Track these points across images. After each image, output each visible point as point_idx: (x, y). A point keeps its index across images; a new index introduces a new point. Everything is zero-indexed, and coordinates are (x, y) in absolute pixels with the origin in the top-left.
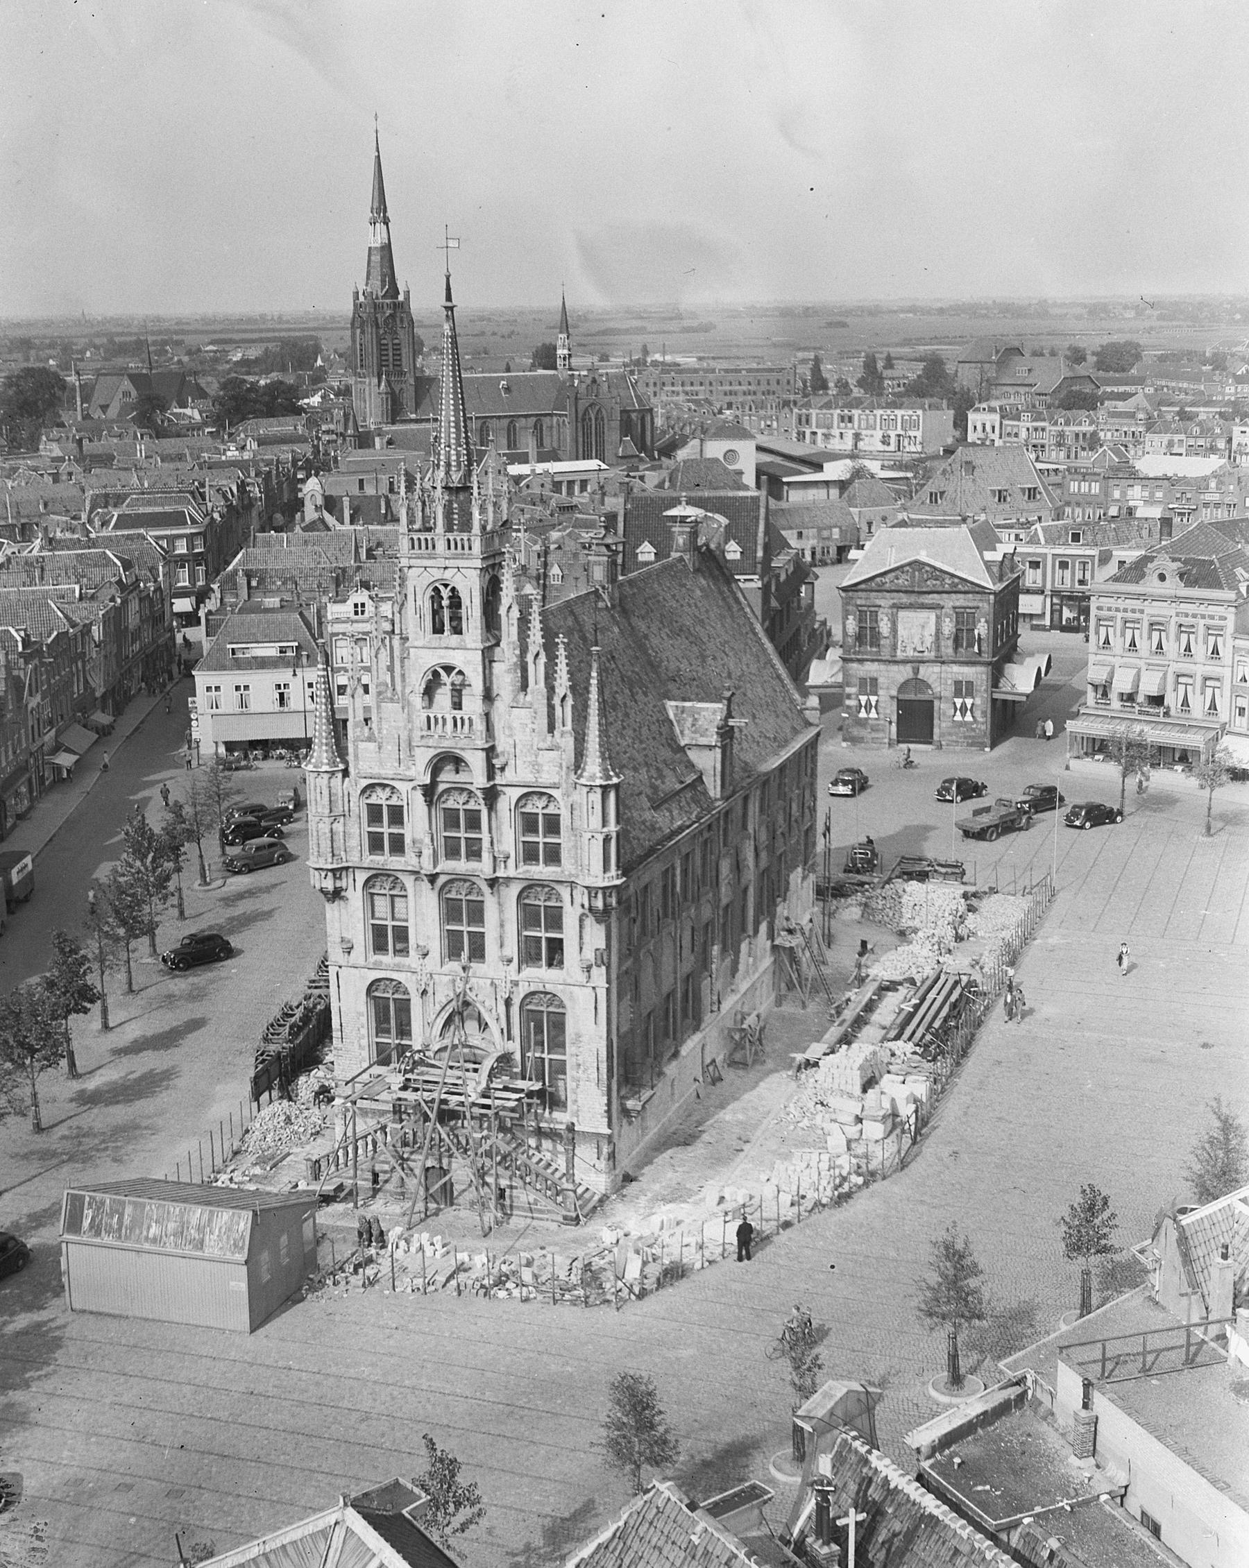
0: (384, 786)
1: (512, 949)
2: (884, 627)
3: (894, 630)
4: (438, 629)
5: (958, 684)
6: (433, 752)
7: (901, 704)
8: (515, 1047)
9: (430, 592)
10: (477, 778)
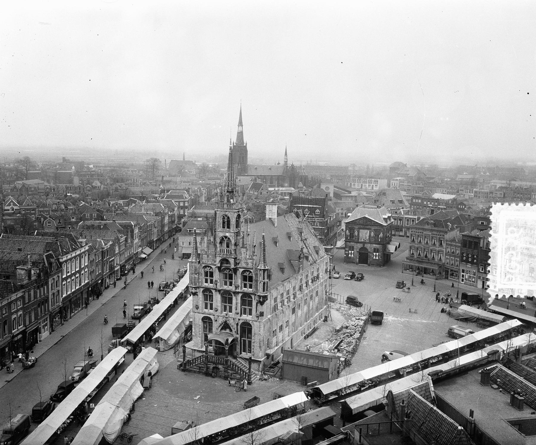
0: (209, 267)
1: (239, 311)
2: (356, 233)
3: (358, 234)
4: (224, 227)
5: (375, 249)
6: (221, 258)
7: (360, 253)
8: (238, 336)
9: (222, 217)
10: (232, 266)
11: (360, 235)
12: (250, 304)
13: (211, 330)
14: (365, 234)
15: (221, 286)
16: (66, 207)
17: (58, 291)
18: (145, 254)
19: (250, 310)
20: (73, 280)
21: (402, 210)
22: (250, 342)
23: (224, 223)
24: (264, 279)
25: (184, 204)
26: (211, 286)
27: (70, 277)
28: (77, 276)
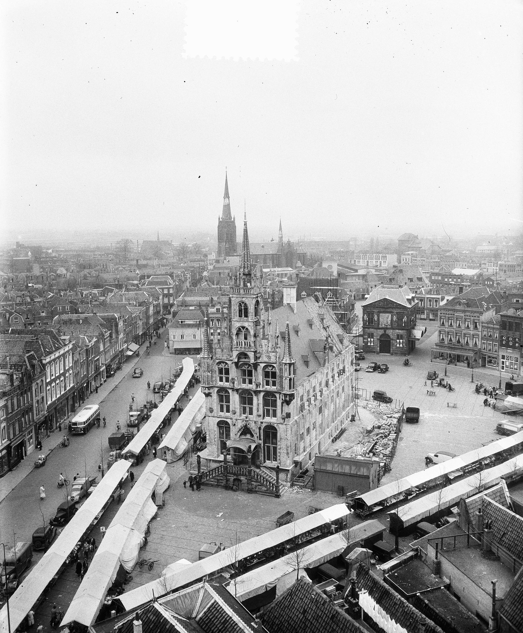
0: (223, 362)
1: (261, 412)
2: (376, 318)
3: (378, 319)
4: (240, 316)
5: (398, 335)
6: (238, 352)
7: (381, 341)
8: (261, 442)
9: (238, 304)
10: (252, 361)
11: (381, 319)
12: (274, 404)
13: (228, 436)
14: (385, 319)
15: (239, 384)
16: (32, 300)
17: (43, 398)
18: (131, 350)
19: (275, 412)
20: (58, 384)
21: (422, 289)
22: (275, 449)
23: (240, 311)
24: (290, 375)
25: (169, 291)
26: (227, 385)
27: (54, 380)
28: (61, 379)
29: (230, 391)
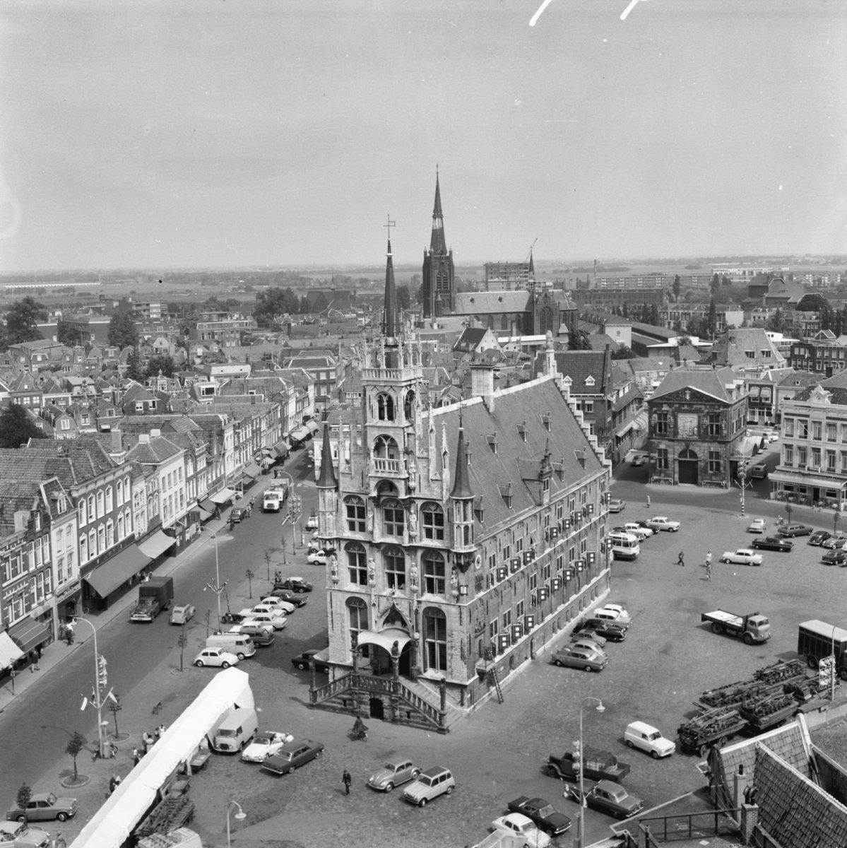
2: (671, 419)
11: (680, 424)
12: (441, 571)
13: (365, 626)
14: (687, 423)
15: (383, 535)
16: (98, 390)
21: (769, 371)
22: (443, 647)
23: (381, 409)
24: (465, 519)
25: (328, 376)
26: (358, 536)
27: (95, 525)
28: (108, 524)
29: (366, 547)
